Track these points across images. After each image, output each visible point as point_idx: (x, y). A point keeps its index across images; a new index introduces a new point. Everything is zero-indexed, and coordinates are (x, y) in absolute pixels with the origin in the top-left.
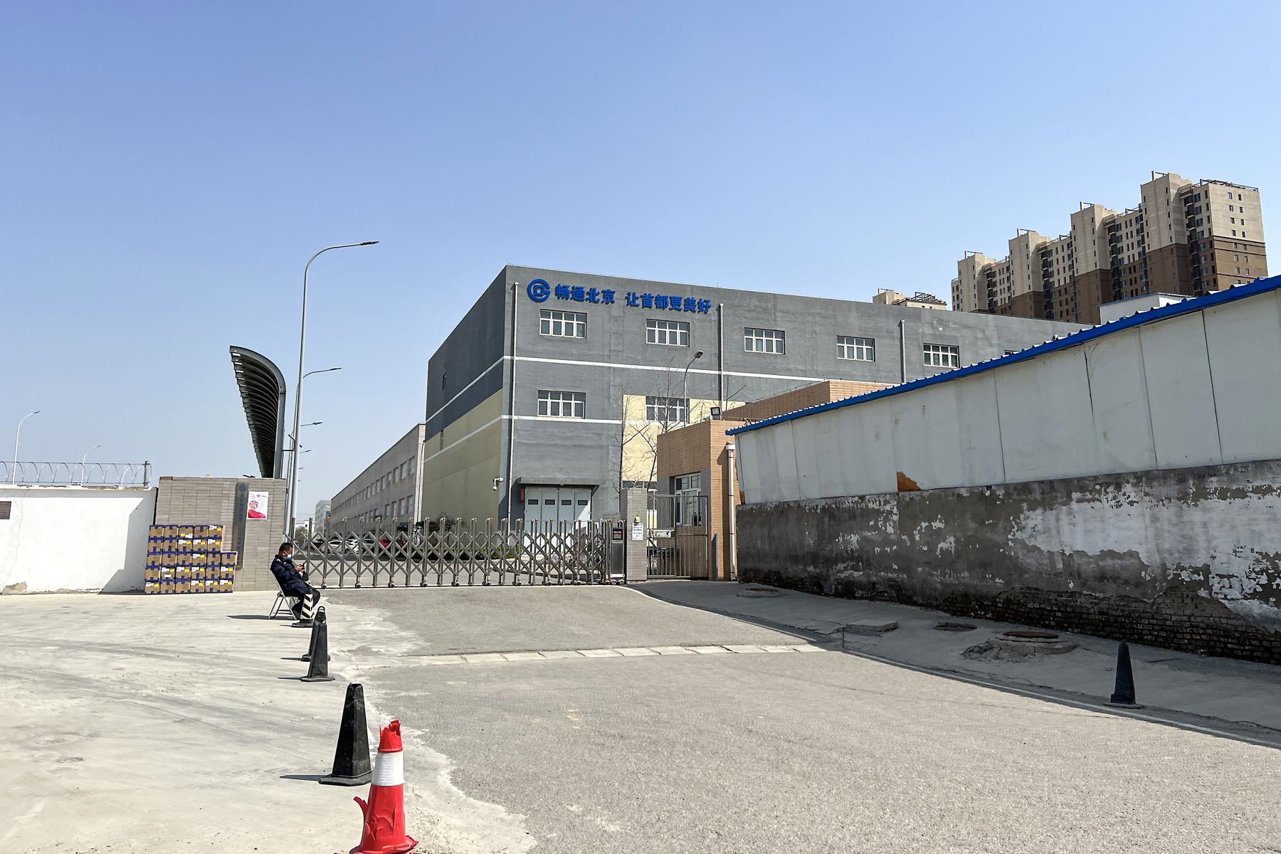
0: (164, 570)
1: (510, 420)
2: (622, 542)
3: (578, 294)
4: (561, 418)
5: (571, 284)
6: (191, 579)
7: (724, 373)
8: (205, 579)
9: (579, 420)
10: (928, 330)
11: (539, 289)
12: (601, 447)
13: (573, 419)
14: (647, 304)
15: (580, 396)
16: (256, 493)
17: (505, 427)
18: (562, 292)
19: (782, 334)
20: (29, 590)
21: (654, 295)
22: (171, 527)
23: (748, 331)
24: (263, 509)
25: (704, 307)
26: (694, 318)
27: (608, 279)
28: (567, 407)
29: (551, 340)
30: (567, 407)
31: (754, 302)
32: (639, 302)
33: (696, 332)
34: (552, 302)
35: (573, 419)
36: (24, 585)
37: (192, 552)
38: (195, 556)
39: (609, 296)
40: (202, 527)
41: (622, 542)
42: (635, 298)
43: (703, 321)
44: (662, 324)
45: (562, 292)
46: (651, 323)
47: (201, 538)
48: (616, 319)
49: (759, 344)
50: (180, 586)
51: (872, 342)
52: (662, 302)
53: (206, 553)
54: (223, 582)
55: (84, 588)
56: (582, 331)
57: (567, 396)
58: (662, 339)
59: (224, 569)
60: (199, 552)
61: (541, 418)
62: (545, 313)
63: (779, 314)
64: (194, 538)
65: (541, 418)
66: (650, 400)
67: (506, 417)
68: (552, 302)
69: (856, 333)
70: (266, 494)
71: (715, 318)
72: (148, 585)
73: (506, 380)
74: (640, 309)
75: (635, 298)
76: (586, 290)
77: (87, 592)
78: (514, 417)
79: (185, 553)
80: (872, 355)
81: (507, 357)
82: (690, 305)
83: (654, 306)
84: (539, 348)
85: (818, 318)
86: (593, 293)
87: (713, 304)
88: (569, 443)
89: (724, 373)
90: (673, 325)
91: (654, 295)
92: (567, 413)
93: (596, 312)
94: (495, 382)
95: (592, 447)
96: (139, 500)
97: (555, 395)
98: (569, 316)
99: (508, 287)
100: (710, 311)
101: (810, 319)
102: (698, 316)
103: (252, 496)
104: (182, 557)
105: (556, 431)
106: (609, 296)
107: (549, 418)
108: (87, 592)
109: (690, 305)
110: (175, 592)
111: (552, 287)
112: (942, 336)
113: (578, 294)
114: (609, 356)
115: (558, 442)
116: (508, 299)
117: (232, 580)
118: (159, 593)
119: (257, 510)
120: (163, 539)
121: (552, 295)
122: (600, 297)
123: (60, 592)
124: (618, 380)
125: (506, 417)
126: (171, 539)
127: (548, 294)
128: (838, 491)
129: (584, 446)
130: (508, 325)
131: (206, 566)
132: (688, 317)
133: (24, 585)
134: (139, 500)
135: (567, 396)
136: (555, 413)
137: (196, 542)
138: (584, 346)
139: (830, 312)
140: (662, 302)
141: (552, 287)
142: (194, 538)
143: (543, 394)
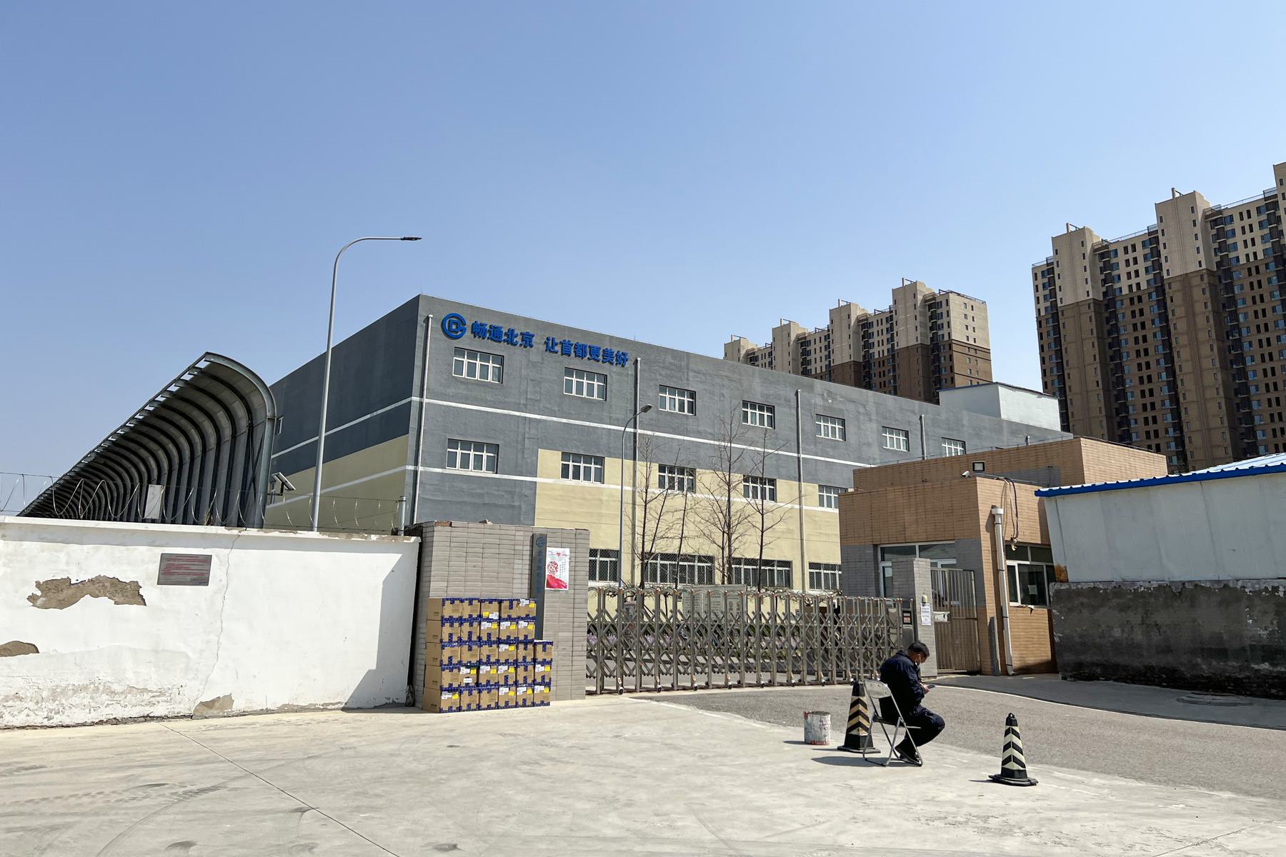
0: (464, 670)
1: (416, 472)
2: (911, 627)
3: (495, 334)
4: (471, 472)
5: (488, 322)
6: (497, 685)
7: (639, 431)
8: (516, 684)
9: (491, 475)
10: (819, 401)
11: (453, 325)
12: (513, 507)
13: (484, 473)
14: (566, 353)
15: (495, 448)
16: (555, 550)
17: (409, 480)
18: (478, 330)
19: (693, 395)
20: (238, 705)
21: (574, 342)
22: (471, 601)
23: (663, 388)
24: (563, 575)
25: (621, 359)
26: (612, 370)
27: (527, 320)
28: (478, 459)
29: (464, 382)
30: (478, 459)
31: (669, 359)
32: (558, 348)
33: (613, 386)
34: (467, 341)
35: (484, 473)
36: (228, 700)
37: (499, 642)
38: (503, 647)
39: (527, 340)
40: (511, 601)
41: (911, 627)
42: (554, 344)
43: (620, 374)
44: (580, 374)
45: (478, 330)
46: (569, 371)
47: (509, 619)
48: (534, 365)
49: (671, 403)
50: (485, 698)
51: (771, 409)
52: (581, 351)
53: (516, 642)
54: (538, 688)
55: (319, 702)
56: (500, 376)
57: (479, 446)
58: (580, 391)
59: (539, 668)
60: (508, 642)
61: (449, 471)
62: (459, 351)
63: (691, 374)
64: (500, 620)
65: (449, 471)
66: (565, 456)
67: (411, 468)
68: (467, 341)
69: (759, 400)
70: (567, 551)
71: (631, 372)
72: (445, 696)
73: (413, 424)
74: (558, 356)
75: (554, 344)
76: (505, 330)
77: (324, 708)
78: (420, 469)
79: (489, 642)
80: (772, 421)
81: (415, 399)
82: (608, 356)
83: (573, 354)
84: (451, 391)
85: (726, 382)
86: (511, 334)
87: (631, 357)
88: (477, 501)
89: (639, 431)
90: (591, 375)
91: (574, 342)
92: (478, 466)
93: (514, 355)
94: (397, 425)
95: (502, 506)
96: (395, 558)
97: (466, 445)
98: (485, 356)
99: (421, 319)
100: (627, 364)
101: (718, 380)
102: (615, 368)
103: (552, 553)
104: (486, 650)
105: (465, 486)
106: (527, 340)
107: (458, 471)
108: (324, 708)
109: (608, 356)
110: (479, 708)
111: (469, 324)
112: (830, 408)
113: (495, 334)
114: (525, 405)
115: (466, 499)
116: (420, 333)
117: (548, 685)
118: (459, 709)
119: (557, 575)
120: (461, 621)
121: (468, 333)
122: (518, 339)
123: (285, 709)
124: (533, 431)
125: (411, 468)
126: (471, 620)
127: (463, 331)
128: (1130, 574)
129: (496, 505)
130: (418, 362)
131: (516, 664)
132: (605, 368)
133: (228, 700)
134: (395, 558)
135: (479, 446)
136: (465, 464)
137: (505, 624)
138: (499, 391)
139: (736, 376)
140: (581, 351)
141: (469, 324)
142: (500, 620)
143: (453, 443)
